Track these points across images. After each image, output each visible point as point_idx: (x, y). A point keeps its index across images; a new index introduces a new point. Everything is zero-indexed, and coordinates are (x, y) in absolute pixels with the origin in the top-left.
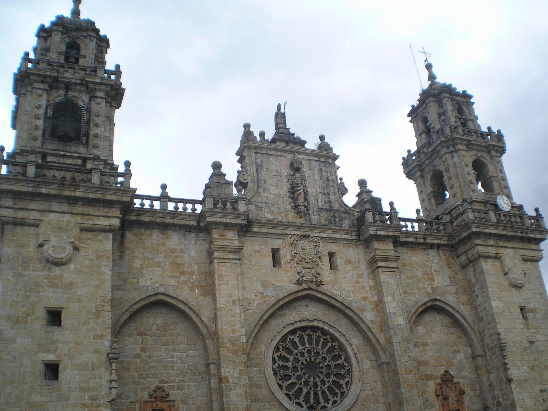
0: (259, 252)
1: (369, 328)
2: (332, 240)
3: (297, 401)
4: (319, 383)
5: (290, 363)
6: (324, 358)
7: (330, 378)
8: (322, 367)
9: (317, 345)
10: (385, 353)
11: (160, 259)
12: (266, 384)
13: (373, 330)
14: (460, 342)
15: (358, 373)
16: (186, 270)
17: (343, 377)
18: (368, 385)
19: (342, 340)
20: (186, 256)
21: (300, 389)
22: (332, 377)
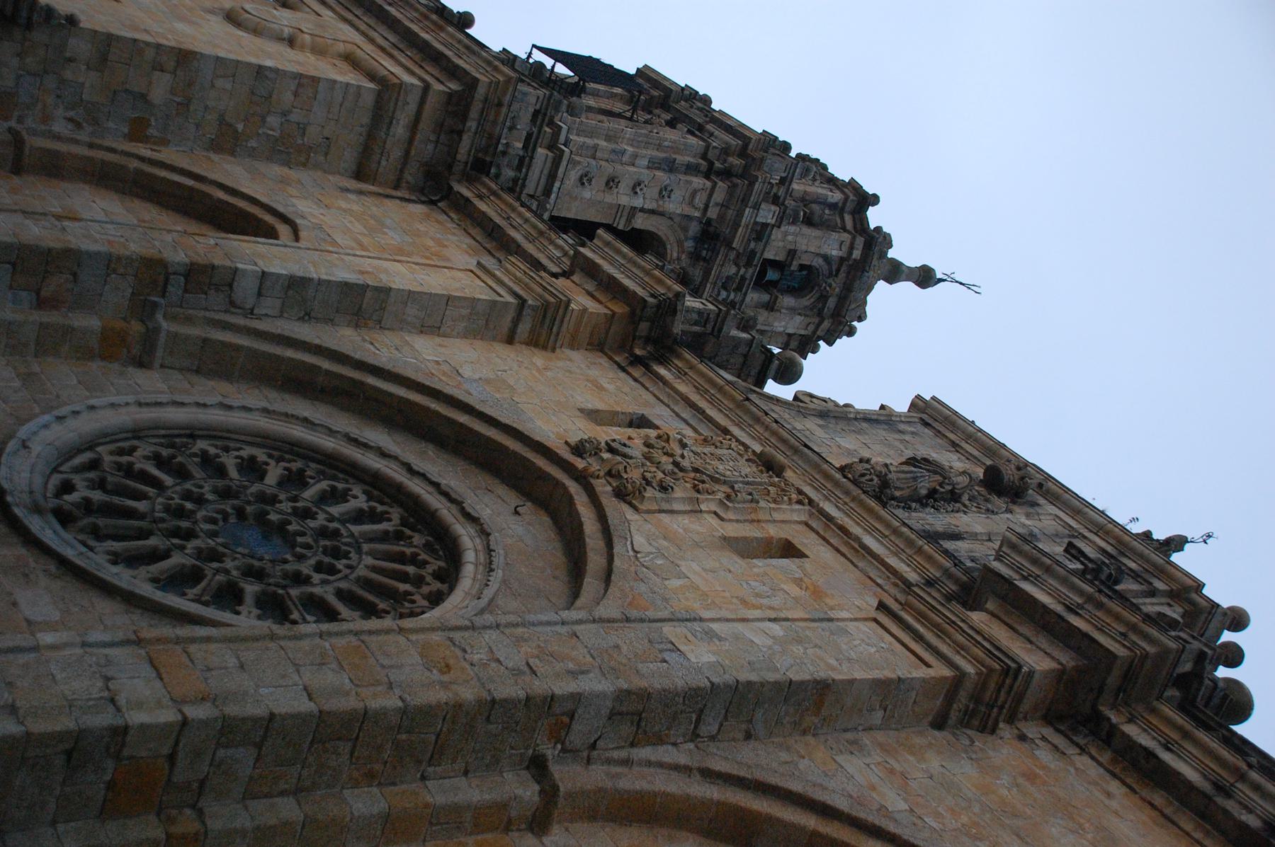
2: (847, 544)
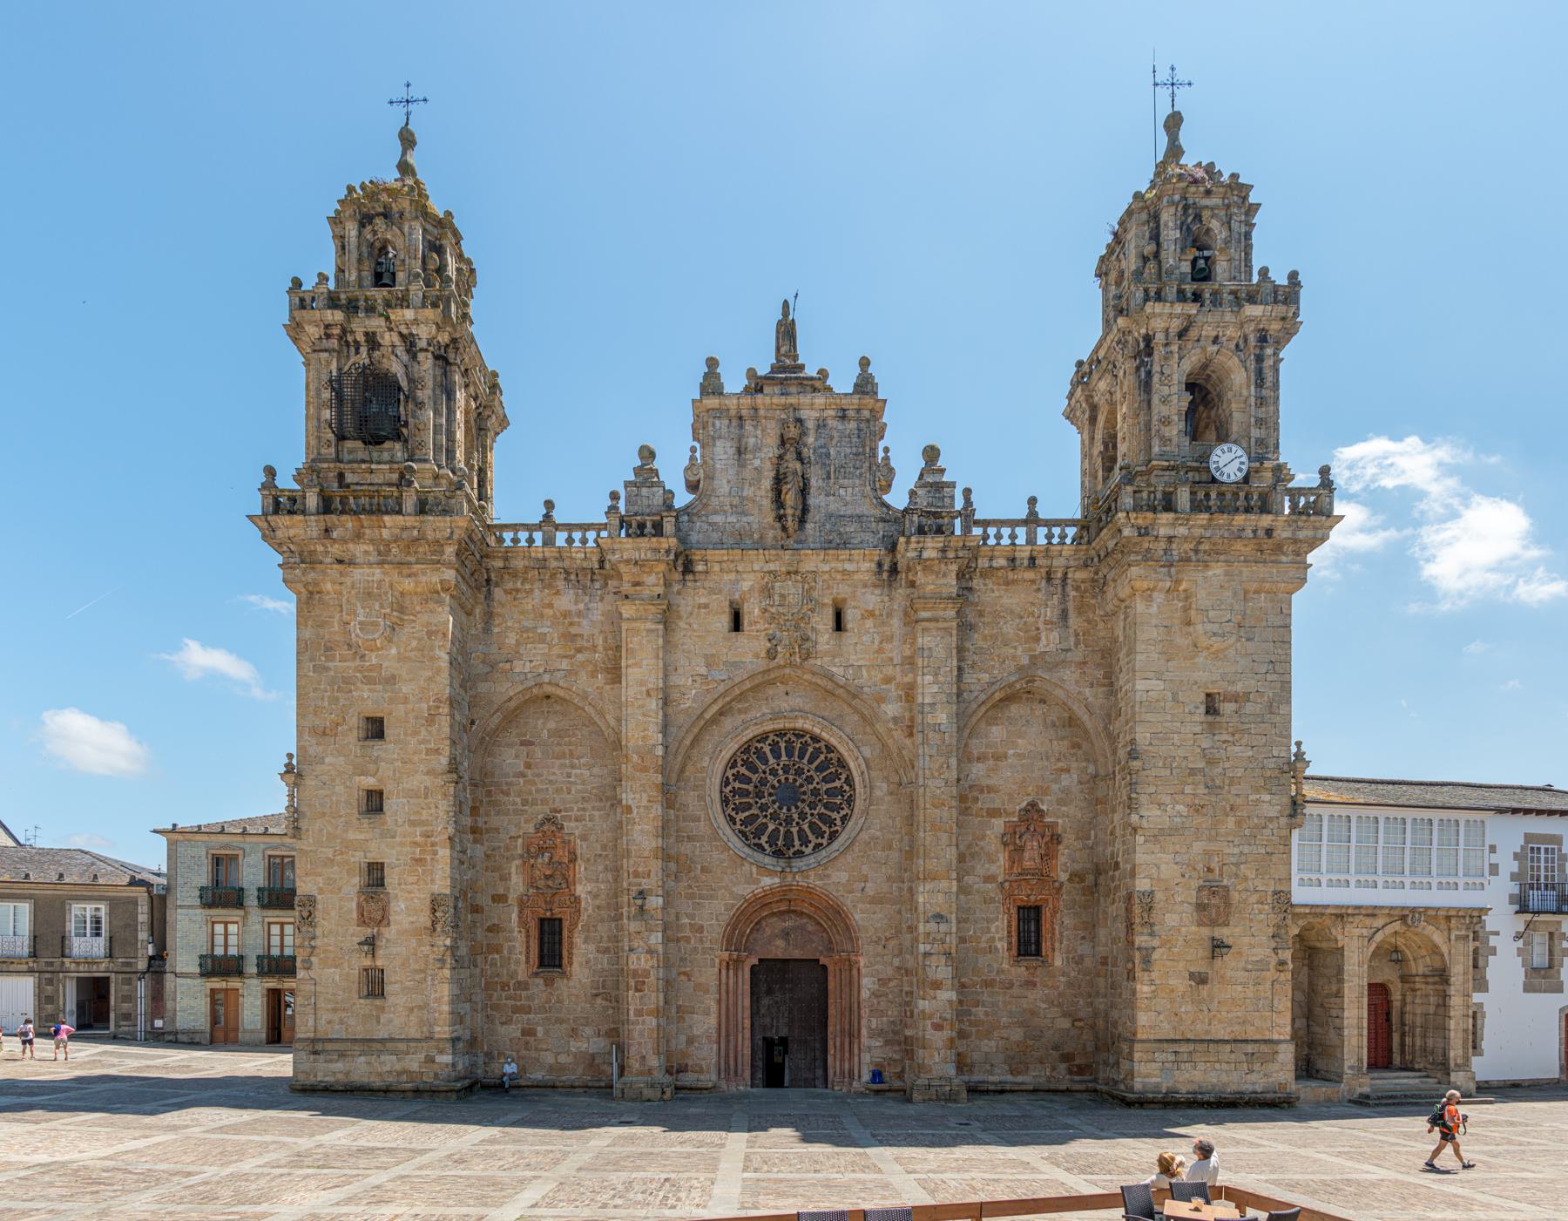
0: (706, 606)
3: (756, 841)
4: (795, 816)
6: (810, 780)
8: (804, 793)
9: (801, 757)
11: (546, 630)
14: (1075, 754)
16: (585, 644)
17: (839, 808)
19: (842, 750)
20: (585, 622)
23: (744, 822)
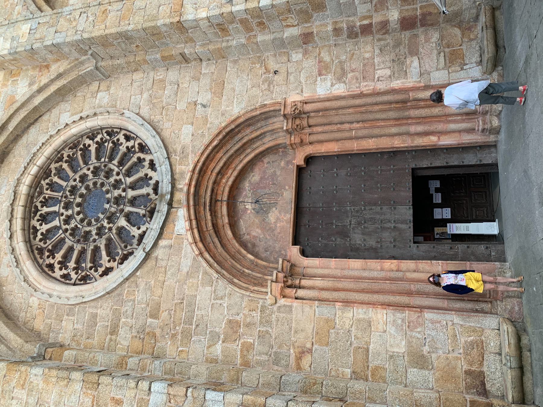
1: (40, 90)
4: (116, 193)
5: (75, 245)
6: (83, 178)
7: (113, 170)
8: (95, 184)
10: (82, 63)
12: (92, 304)
13: (42, 84)
15: (111, 116)
18: (133, 97)
19: (57, 142)
21: (121, 230)
22: (112, 167)
23: (111, 255)
